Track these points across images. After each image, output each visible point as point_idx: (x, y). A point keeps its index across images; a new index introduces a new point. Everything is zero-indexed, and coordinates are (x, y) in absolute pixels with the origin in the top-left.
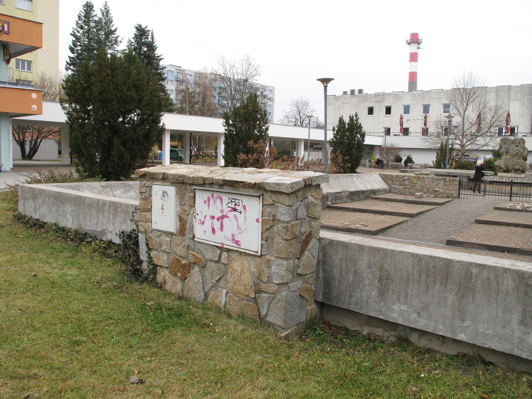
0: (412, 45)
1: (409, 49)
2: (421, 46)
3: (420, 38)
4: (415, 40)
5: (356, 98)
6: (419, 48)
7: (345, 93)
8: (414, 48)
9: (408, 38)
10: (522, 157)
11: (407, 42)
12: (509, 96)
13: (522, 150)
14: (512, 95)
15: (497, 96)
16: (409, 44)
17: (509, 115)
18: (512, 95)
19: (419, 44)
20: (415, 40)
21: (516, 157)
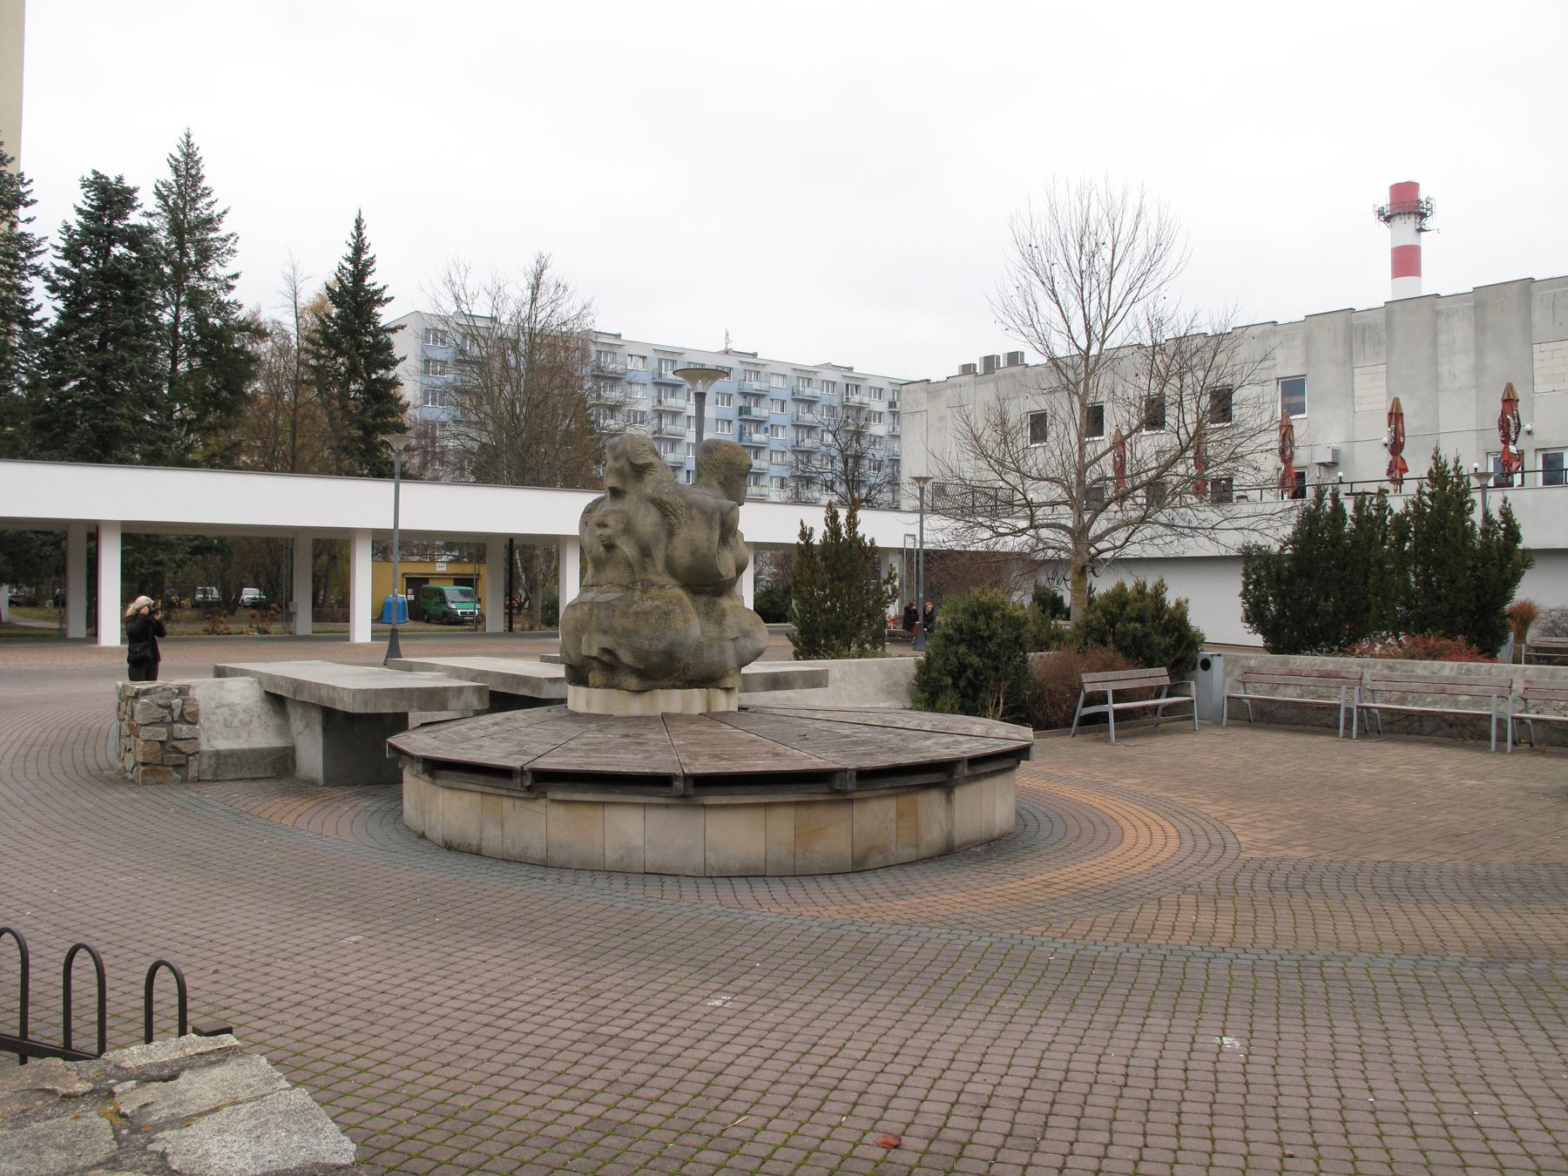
0: (1398, 222)
1: (1384, 239)
2: (1428, 223)
3: (1422, 197)
4: (1406, 204)
5: (992, 386)
6: (1420, 230)
7: (967, 369)
8: (1404, 231)
9: (1384, 200)
10: (671, 569)
11: (1380, 213)
12: (1527, 324)
13: (647, 521)
14: (1539, 316)
15: (1480, 328)
16: (1388, 219)
17: (1510, 401)
18: (1537, 317)
19: (1423, 216)
20: (1406, 204)
21: (610, 574)
